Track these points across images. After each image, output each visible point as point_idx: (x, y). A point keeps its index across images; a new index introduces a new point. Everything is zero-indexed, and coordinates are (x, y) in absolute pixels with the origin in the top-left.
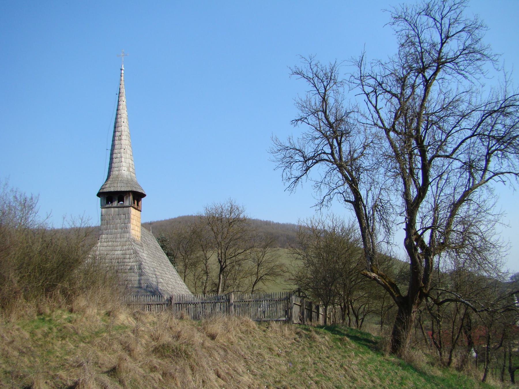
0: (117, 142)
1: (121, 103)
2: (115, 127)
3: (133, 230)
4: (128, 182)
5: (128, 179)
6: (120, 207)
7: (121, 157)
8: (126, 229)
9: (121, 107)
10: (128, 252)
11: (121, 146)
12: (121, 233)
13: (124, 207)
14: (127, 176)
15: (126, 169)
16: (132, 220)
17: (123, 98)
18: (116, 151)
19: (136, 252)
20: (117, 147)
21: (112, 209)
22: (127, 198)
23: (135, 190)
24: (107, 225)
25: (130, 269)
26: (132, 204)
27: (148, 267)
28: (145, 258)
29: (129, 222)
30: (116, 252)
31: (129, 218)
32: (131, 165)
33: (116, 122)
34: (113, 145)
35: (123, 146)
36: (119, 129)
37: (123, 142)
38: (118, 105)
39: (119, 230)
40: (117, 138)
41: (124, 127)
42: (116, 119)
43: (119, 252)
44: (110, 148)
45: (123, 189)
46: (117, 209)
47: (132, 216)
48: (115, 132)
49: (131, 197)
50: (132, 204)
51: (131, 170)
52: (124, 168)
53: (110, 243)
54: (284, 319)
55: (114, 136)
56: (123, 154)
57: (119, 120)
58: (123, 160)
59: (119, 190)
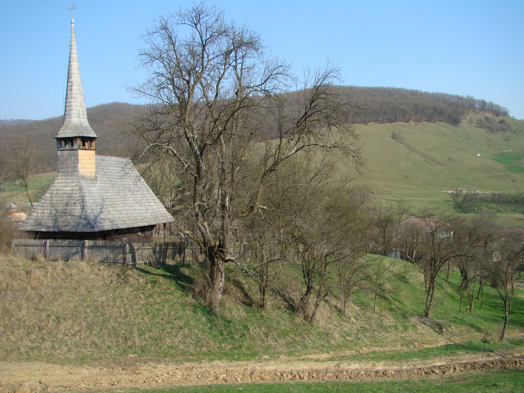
0: (69, 92)
1: (72, 55)
2: (68, 78)
3: (82, 168)
4: (76, 128)
5: (77, 125)
6: (71, 150)
7: (72, 106)
8: (75, 169)
9: (72, 59)
10: (75, 188)
11: (72, 96)
12: (72, 172)
13: (73, 150)
14: (76, 122)
15: (76, 116)
16: (80, 161)
17: (74, 51)
18: (68, 100)
19: (81, 189)
20: (69, 96)
21: (65, 151)
22: (75, 142)
23: (81, 135)
24: (62, 165)
25: (75, 203)
26: (79, 147)
27: (91, 201)
28: (95, 191)
29: (78, 163)
30: (67, 188)
31: (77, 159)
32: (81, 112)
33: (69, 73)
34: (67, 95)
35: (74, 96)
36: (70, 80)
37: (74, 91)
38: (70, 57)
39: (71, 169)
40: (69, 88)
41: (76, 78)
42: (69, 70)
43: (69, 188)
44: (65, 97)
45: (70, 136)
46: (68, 152)
47: (80, 157)
48: (68, 82)
49: (79, 142)
50: (79, 147)
51: (81, 116)
52: (74, 116)
53: (64, 181)
54: (122, 262)
55: (67, 87)
56: (73, 104)
57: (70, 71)
58: (73, 108)
59: (67, 136)
